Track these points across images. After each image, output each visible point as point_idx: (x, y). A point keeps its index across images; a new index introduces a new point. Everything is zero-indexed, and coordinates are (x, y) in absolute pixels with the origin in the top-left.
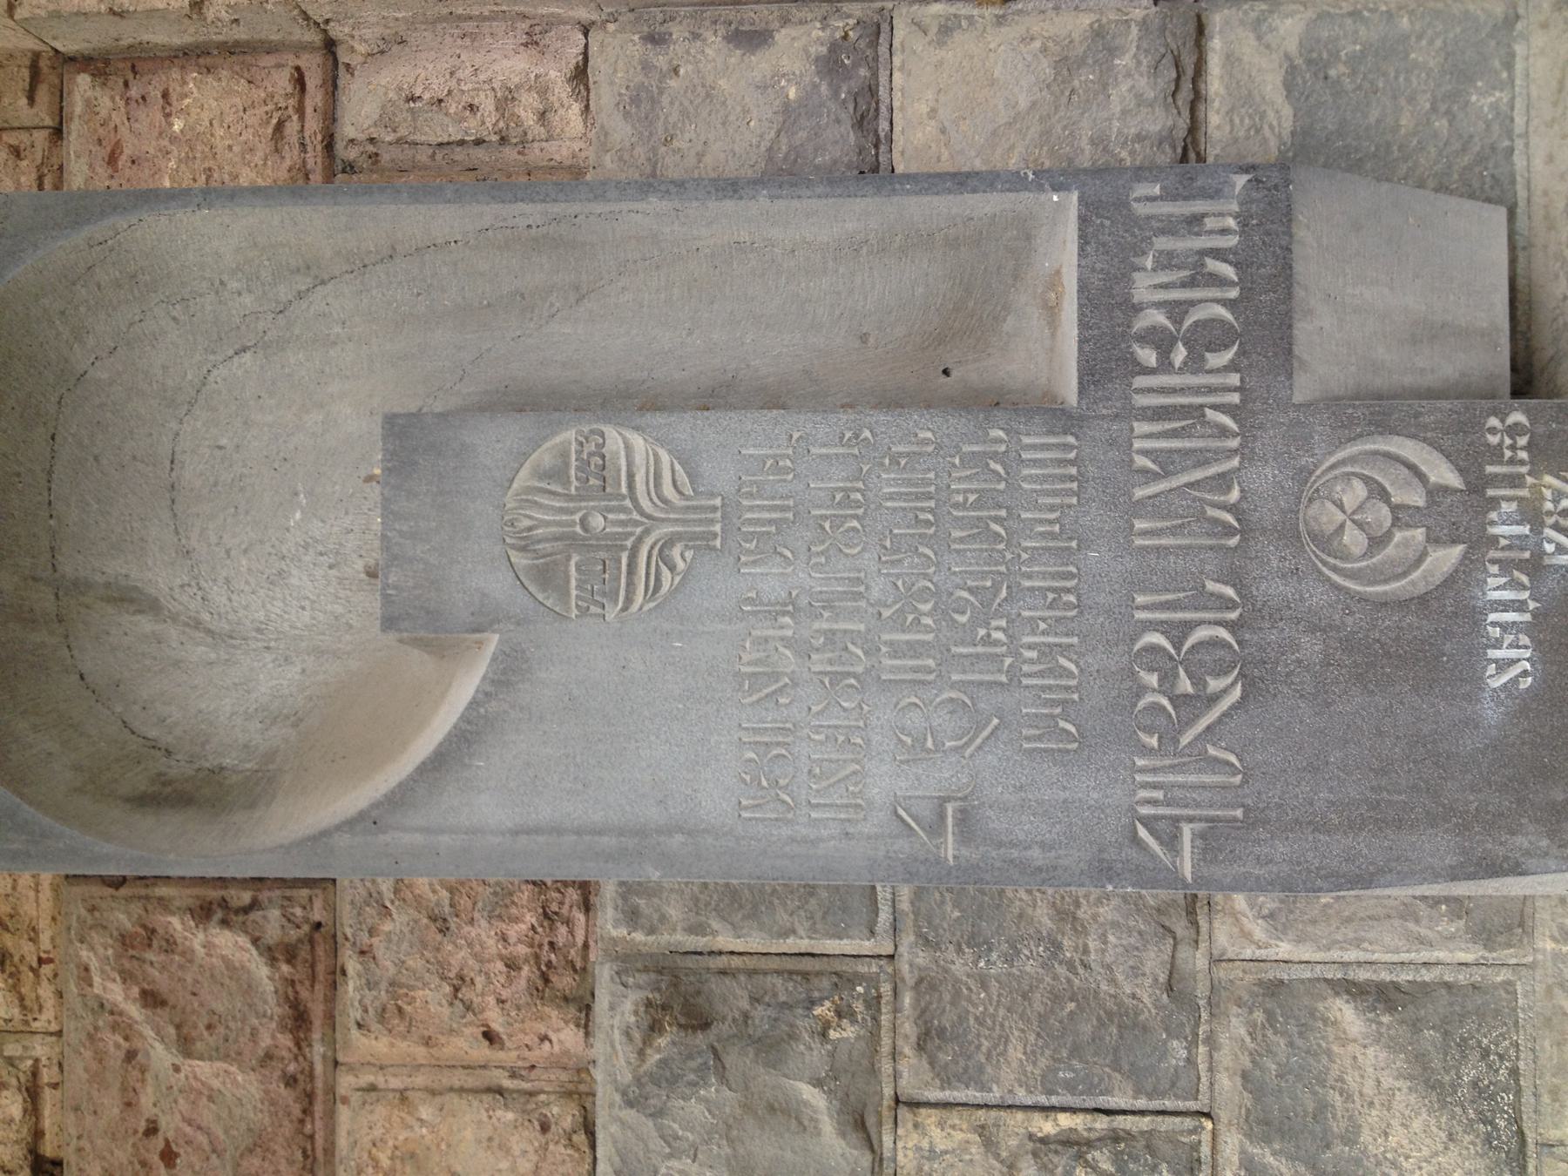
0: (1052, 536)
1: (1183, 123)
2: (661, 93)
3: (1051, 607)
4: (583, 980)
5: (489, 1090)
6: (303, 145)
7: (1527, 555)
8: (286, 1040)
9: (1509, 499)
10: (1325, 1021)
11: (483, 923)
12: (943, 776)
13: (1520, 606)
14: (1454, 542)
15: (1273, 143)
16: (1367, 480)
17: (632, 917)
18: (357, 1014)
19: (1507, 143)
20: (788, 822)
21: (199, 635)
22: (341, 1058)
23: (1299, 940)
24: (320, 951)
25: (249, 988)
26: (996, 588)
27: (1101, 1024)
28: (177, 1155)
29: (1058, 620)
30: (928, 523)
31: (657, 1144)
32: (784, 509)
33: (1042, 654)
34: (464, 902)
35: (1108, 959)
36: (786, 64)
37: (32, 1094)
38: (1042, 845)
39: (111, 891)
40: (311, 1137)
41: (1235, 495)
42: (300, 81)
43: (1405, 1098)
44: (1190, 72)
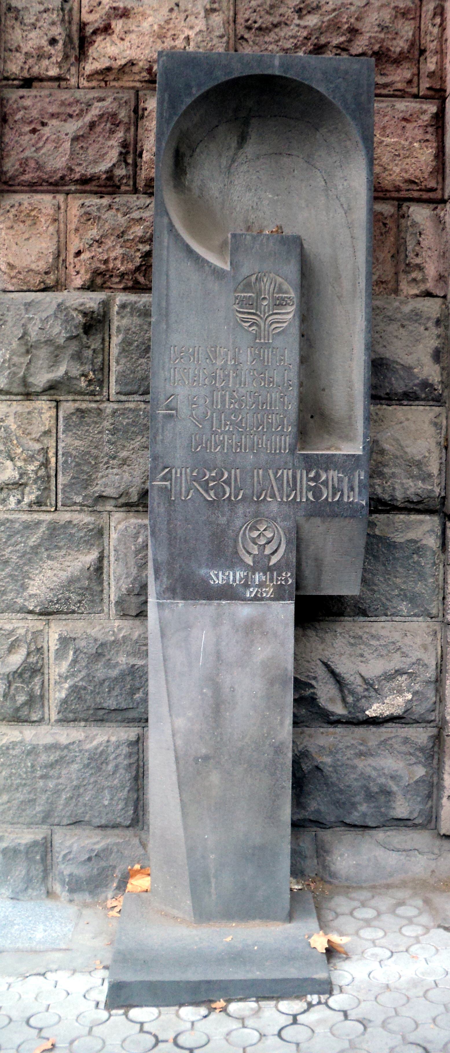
0: (258, 444)
2: (420, 324)
3: (236, 444)
4: (99, 287)
5: (59, 252)
8: (77, 176)
9: (266, 578)
10: (90, 549)
13: (234, 580)
14: (254, 562)
15: (392, 536)
16: (273, 536)
17: (123, 306)
18: (87, 204)
20: (170, 361)
21: (230, 162)
22: (70, 196)
23: (119, 540)
24: (109, 189)
25: (95, 162)
26: (242, 427)
27: (87, 473)
28: (34, 134)
30: (262, 407)
31: (44, 315)
32: (268, 362)
34: (128, 244)
35: (110, 476)
36: (426, 369)
37: (58, 79)
38: (163, 440)
39: (132, 108)
40: (41, 185)
41: (269, 499)
43: (64, 576)
44: (417, 507)
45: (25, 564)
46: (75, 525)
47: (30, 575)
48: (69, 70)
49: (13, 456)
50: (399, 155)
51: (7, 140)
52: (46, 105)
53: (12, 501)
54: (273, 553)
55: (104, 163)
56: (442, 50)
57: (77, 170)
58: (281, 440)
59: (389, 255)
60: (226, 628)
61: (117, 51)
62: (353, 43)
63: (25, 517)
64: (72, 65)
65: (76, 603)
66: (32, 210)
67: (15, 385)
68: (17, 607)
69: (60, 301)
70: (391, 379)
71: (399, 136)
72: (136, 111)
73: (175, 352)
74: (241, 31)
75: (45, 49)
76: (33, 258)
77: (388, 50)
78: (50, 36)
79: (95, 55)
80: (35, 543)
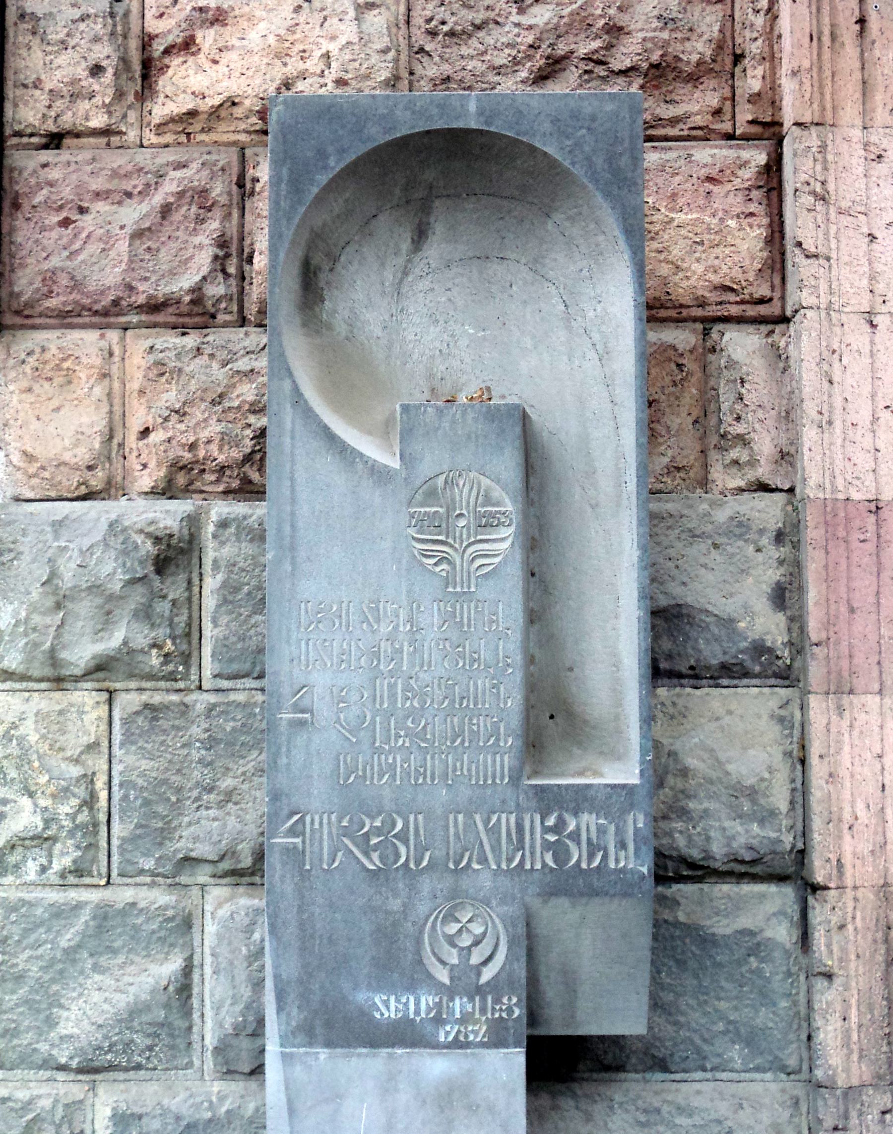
0: (455, 770)
1: (717, 865)
2: (746, 541)
4: (182, 491)
5: (111, 430)
6: (721, 303)
7: (444, 1016)
8: (141, 299)
9: (474, 1007)
10: (167, 953)
11: (219, 429)
12: (324, 711)
13: (417, 1012)
14: (452, 979)
16: (484, 934)
17: (223, 524)
19: (709, 1066)
20: (299, 627)
21: (399, 275)
22: (129, 333)
23: (220, 937)
24: (197, 319)
25: (173, 273)
26: (425, 740)
28: (67, 228)
29: (409, 774)
30: (461, 705)
31: (86, 543)
32: (469, 626)
33: (391, 765)
34: (231, 416)
35: (202, 822)
36: (760, 621)
37: (106, 132)
38: (289, 764)
39: (235, 179)
40: (79, 315)
41: (476, 866)
42: (762, 301)
43: (122, 1001)
45: (53, 981)
46: (142, 910)
47: (63, 1001)
48: (125, 116)
49: (33, 789)
50: (702, 243)
51: (19, 240)
52: (86, 178)
53: (31, 868)
54: (486, 962)
55: (187, 276)
56: (773, 56)
57: (141, 289)
58: (494, 761)
59: (690, 420)
60: (404, 1097)
61: (206, 83)
62: (614, 50)
63: (53, 896)
64: (129, 107)
65: (143, 1051)
66: (64, 360)
67: (36, 664)
68: (37, 1059)
69: (113, 516)
70: (696, 640)
71: (701, 209)
72: (241, 185)
73: (307, 612)
74: (420, 38)
75: (83, 83)
76: (67, 442)
77: (677, 59)
78: (91, 62)
79: (169, 90)
80: (72, 943)
